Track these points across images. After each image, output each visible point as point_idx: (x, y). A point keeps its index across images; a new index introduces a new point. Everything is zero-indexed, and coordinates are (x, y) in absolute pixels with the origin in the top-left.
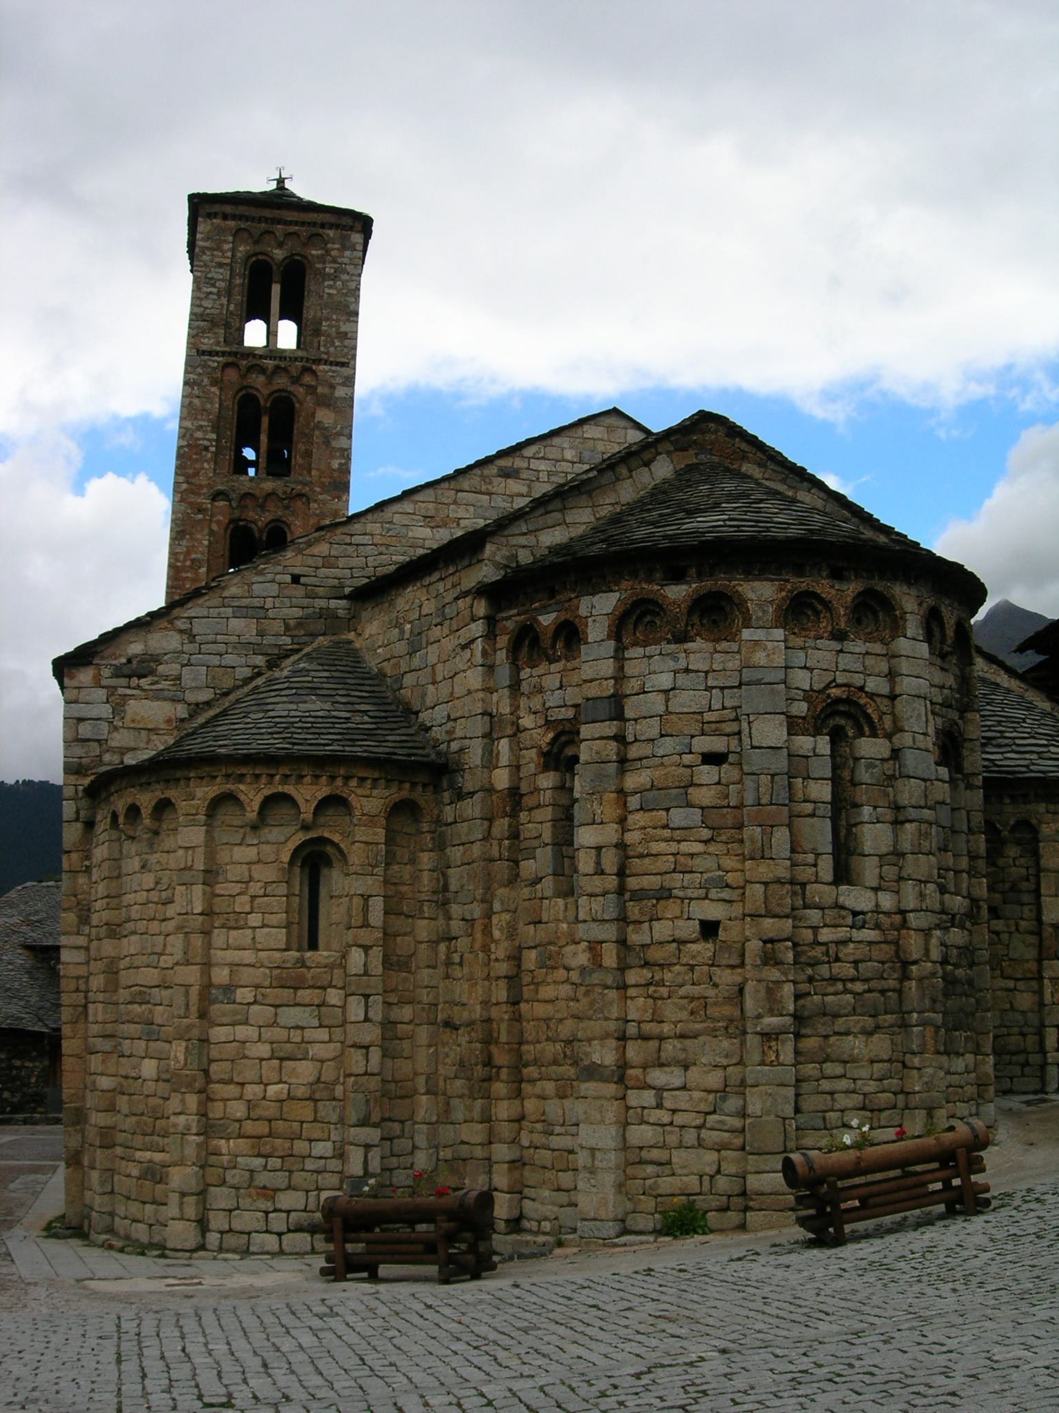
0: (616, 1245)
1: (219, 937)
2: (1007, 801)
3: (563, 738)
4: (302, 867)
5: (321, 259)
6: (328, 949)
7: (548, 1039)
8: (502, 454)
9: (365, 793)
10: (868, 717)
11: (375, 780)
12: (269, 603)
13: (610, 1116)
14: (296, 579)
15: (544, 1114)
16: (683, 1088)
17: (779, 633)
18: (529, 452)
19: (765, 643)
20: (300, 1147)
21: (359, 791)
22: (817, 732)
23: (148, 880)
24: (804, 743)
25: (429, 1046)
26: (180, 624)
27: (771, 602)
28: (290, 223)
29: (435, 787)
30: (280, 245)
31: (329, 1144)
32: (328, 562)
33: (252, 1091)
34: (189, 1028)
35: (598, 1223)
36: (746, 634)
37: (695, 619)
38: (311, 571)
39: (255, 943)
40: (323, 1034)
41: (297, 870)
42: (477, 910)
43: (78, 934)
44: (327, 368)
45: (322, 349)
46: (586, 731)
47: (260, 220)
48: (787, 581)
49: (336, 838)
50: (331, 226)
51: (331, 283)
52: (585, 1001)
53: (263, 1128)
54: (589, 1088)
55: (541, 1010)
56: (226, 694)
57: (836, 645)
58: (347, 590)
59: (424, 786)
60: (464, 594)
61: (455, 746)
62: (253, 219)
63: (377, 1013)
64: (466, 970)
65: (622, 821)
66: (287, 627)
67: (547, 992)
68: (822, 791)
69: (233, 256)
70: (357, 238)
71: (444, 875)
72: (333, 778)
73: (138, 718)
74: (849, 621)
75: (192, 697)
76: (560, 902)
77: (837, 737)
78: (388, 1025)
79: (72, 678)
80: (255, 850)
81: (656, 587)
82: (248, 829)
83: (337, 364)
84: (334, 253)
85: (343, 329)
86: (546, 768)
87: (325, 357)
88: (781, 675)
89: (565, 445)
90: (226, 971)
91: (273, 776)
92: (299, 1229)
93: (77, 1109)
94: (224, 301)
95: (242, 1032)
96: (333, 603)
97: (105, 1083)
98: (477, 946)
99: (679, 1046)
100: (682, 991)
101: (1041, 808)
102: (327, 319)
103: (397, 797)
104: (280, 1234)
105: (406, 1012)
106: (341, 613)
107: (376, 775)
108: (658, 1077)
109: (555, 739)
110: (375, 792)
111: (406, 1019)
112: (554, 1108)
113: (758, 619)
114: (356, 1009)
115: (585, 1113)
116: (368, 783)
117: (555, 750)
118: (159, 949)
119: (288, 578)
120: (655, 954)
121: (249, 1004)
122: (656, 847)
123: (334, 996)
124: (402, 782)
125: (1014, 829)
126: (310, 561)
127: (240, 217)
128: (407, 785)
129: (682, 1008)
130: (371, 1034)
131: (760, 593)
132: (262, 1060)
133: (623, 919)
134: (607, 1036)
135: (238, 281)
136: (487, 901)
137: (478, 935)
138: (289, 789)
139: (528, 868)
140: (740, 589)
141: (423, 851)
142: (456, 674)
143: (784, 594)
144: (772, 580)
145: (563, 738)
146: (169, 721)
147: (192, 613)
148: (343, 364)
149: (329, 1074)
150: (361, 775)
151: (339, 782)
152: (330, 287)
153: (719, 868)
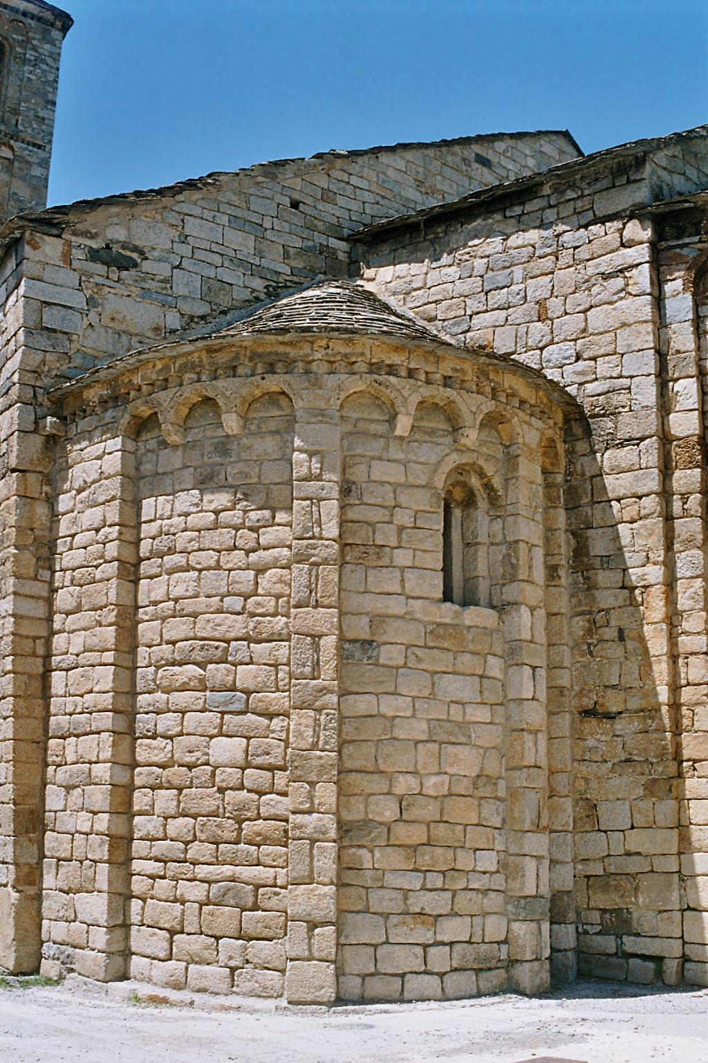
5: (25, 43)
8: (480, 139)
12: (267, 224)
14: (295, 205)
18: (500, 146)
26: (173, 218)
32: (327, 196)
33: (404, 784)
38: (309, 200)
43: (35, 578)
44: (24, 146)
45: (20, 127)
51: (32, 69)
53: (417, 835)
56: (224, 313)
58: (346, 232)
60: (603, 220)
73: (120, 317)
75: (187, 308)
79: (35, 247)
83: (34, 145)
84: (35, 42)
85: (41, 114)
87: (23, 135)
89: (528, 152)
96: (334, 243)
102: (26, 101)
106: (342, 256)
118: (247, 587)
119: (287, 201)
121: (398, 668)
126: (309, 189)
132: (417, 742)
142: (591, 307)
146: (157, 329)
147: (185, 208)
148: (39, 147)
149: (493, 767)
152: (31, 72)
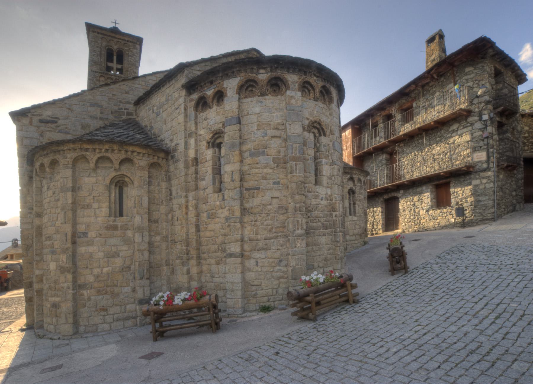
1: (80, 213)
3: (216, 136)
4: (116, 186)
6: (127, 216)
9: (141, 158)
10: (323, 129)
11: (144, 154)
13: (239, 270)
21: (137, 157)
23: (50, 193)
25: (166, 249)
28: (118, 39)
29: (167, 160)
30: (116, 44)
34: (67, 249)
37: (269, 87)
39: (97, 215)
40: (125, 248)
41: (113, 187)
42: (183, 200)
46: (226, 130)
47: (109, 36)
49: (129, 175)
50: (130, 42)
52: (228, 229)
54: (230, 260)
55: (208, 234)
59: (163, 159)
61: (173, 144)
62: (107, 35)
63: (147, 239)
64: (179, 222)
65: (241, 161)
66: (112, 113)
67: (211, 227)
68: (311, 152)
69: (101, 45)
70: (138, 46)
71: (170, 190)
72: (127, 151)
76: (216, 195)
78: (151, 244)
80: (95, 179)
81: (254, 75)
82: (91, 171)
86: (208, 148)
90: (84, 226)
91: (101, 149)
93: (30, 282)
94: (99, 57)
95: (91, 249)
96: (127, 106)
97: (37, 272)
98: (184, 213)
103: (152, 161)
105: (158, 238)
107: (144, 152)
109: (213, 137)
110: (144, 158)
111: (158, 241)
114: (138, 238)
116: (141, 155)
117: (212, 140)
120: (256, 210)
122: (254, 171)
123: (129, 233)
124: (154, 156)
127: (103, 34)
128: (156, 157)
130: (145, 246)
133: (242, 197)
134: (237, 241)
135: (103, 53)
136: (186, 197)
137: (184, 210)
138: (109, 155)
139: (202, 184)
141: (162, 181)
145: (216, 136)
150: (138, 151)
151: (129, 153)
153: (279, 178)
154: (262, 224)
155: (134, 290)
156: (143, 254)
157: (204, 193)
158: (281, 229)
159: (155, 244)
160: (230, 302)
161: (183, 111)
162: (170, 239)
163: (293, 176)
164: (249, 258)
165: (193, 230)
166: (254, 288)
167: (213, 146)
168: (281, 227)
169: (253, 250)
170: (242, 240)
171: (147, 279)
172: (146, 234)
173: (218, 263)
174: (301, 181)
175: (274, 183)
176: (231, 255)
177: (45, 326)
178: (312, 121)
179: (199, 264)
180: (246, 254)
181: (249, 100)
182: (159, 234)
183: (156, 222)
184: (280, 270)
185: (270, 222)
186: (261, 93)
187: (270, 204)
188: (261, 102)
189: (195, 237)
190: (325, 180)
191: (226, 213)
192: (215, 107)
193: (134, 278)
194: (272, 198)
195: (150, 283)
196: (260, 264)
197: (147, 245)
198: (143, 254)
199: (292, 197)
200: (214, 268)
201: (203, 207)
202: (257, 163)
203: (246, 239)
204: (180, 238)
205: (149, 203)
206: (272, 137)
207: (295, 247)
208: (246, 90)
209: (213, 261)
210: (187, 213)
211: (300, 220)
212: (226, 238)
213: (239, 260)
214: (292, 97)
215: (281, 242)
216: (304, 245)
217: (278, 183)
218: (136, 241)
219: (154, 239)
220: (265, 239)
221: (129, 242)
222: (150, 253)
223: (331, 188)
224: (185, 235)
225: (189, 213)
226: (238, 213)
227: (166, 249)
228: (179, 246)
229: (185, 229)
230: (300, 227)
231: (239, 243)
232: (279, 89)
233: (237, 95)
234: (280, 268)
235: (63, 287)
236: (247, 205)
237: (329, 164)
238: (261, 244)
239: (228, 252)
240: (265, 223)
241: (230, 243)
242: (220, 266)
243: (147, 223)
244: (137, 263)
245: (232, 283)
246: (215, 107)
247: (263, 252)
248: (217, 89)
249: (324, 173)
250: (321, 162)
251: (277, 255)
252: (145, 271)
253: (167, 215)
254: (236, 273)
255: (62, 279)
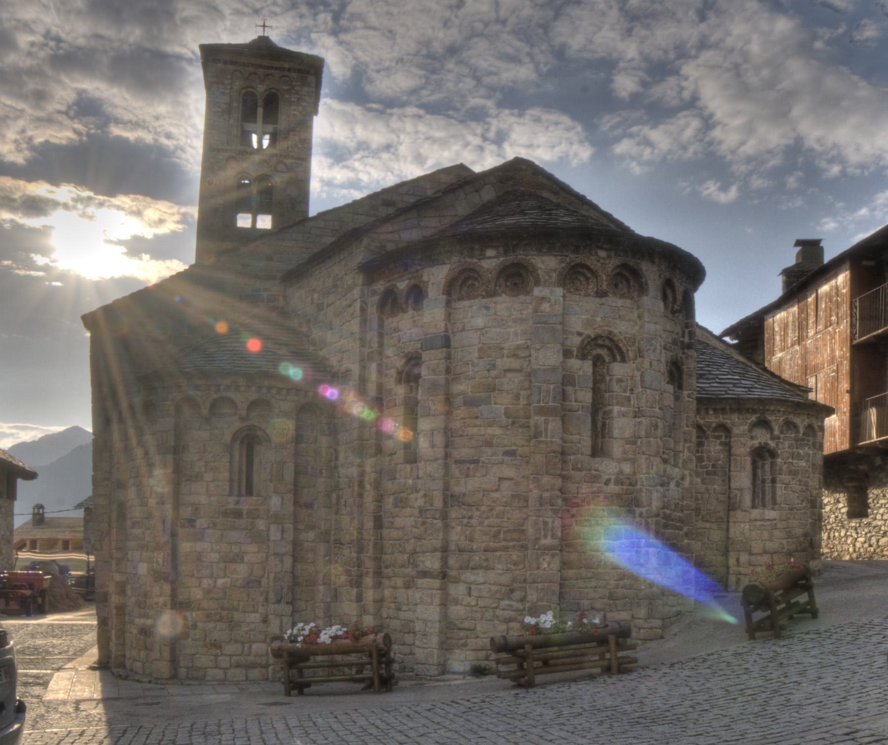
0: (438, 680)
2: (711, 412)
7: (400, 552)
13: (437, 601)
15: (395, 598)
16: (485, 583)
17: (559, 291)
19: (550, 296)
20: (237, 616)
22: (583, 357)
24: (574, 363)
27: (555, 270)
31: (258, 615)
35: (427, 667)
36: (537, 291)
40: (253, 548)
48: (567, 256)
52: (422, 529)
55: (395, 534)
57: (598, 300)
63: (290, 536)
64: (348, 509)
68: (586, 397)
74: (608, 285)
77: (597, 361)
78: (296, 544)
88: (560, 319)
92: (238, 666)
98: (355, 494)
99: (483, 557)
100: (486, 522)
101: (735, 417)
104: (225, 669)
108: (469, 576)
112: (402, 594)
113: (546, 281)
114: (275, 533)
115: (421, 598)
125: (715, 430)
129: (486, 534)
131: (546, 263)
134: (435, 550)
137: (356, 488)
140: (533, 261)
143: (564, 265)
144: (556, 256)
153: (515, 444)
154: (481, 523)
155: (265, 620)
156: (282, 561)
157: (390, 461)
158: (515, 535)
159: (306, 544)
160: (420, 654)
161: (358, 312)
162: (332, 538)
163: (540, 442)
164: (457, 581)
165: (369, 524)
166: (462, 634)
167: (408, 381)
168: (514, 531)
169: (466, 567)
170: (445, 550)
171: (287, 603)
172: (289, 526)
173: (407, 586)
174: (554, 452)
175: (506, 453)
176: (424, 574)
177: (128, 663)
178: (589, 336)
179: (378, 585)
180: (453, 573)
181: (466, 303)
182: (312, 527)
183: (309, 506)
184: (511, 606)
185: (496, 521)
186: (487, 293)
187: (497, 490)
188: (487, 308)
189: (373, 538)
190: (617, 448)
191: (420, 502)
192: (410, 312)
193: (267, 600)
194: (501, 479)
195: (293, 611)
196: (475, 593)
197: (289, 547)
198: (282, 561)
199: (536, 480)
200: (402, 594)
201: (389, 486)
202: (477, 417)
203: (452, 547)
204: (348, 537)
205: (297, 473)
206: (505, 371)
207: (538, 568)
208: (461, 286)
209: (399, 582)
210: (361, 495)
211: (550, 520)
212: (419, 544)
213: (436, 583)
214: (543, 299)
215: (514, 557)
216: (556, 564)
217: (513, 454)
218: (272, 538)
219: (303, 536)
220: (485, 551)
221: (260, 539)
222: (295, 559)
223: (633, 461)
224: (355, 533)
225: (366, 494)
226: (438, 503)
227: (325, 556)
228: (346, 552)
229: (356, 522)
230: (550, 533)
231: (438, 554)
232: (523, 281)
233: (445, 297)
234: (511, 603)
235: (157, 603)
236: (457, 489)
237: (631, 414)
238: (476, 559)
239: (421, 567)
240: (486, 522)
241: (424, 552)
242: (410, 592)
243: (292, 508)
244: (272, 576)
245: (425, 621)
246: (410, 312)
247: (481, 572)
248: (413, 282)
249: (616, 433)
250: (610, 412)
251: (505, 579)
252: (285, 590)
253: (328, 495)
254: (431, 604)
255: (156, 590)
